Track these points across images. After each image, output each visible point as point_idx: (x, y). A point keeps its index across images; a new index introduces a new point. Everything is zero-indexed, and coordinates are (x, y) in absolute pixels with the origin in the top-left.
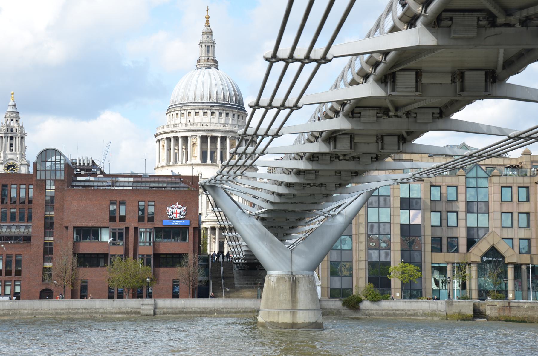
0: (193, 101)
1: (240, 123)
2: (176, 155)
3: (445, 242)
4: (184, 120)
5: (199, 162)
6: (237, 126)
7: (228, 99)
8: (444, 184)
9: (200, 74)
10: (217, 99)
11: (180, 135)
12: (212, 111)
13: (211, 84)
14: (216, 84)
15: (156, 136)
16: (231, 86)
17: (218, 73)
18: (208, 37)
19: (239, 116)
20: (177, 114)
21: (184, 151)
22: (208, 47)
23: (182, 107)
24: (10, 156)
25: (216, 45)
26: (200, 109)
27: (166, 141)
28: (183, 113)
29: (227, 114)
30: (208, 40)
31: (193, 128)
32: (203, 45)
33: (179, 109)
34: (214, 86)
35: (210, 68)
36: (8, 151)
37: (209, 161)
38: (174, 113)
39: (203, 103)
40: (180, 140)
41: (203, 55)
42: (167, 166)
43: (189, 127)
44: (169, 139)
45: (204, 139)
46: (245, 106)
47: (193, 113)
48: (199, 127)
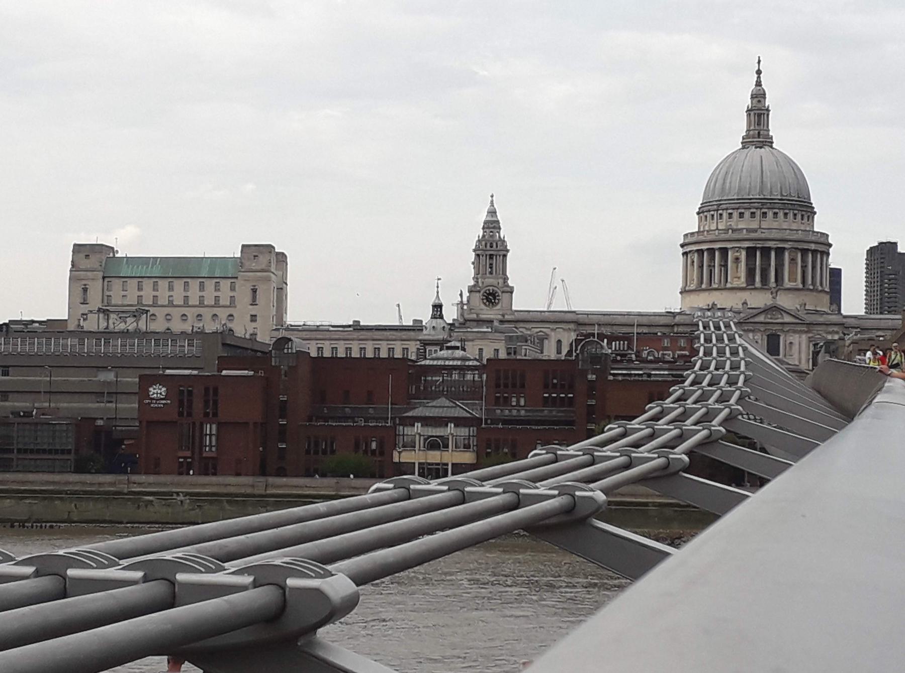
0: (735, 197)
18: (759, 101)
19: (802, 216)
20: (713, 216)
22: (759, 115)
24: (490, 281)
27: (696, 255)
29: (786, 214)
30: (759, 105)
31: (736, 236)
32: (752, 113)
34: (767, 173)
35: (761, 148)
36: (488, 275)
37: (758, 284)
38: (708, 215)
40: (717, 253)
44: (700, 252)
45: (751, 252)
46: (812, 201)
47: (736, 214)
48: (744, 235)
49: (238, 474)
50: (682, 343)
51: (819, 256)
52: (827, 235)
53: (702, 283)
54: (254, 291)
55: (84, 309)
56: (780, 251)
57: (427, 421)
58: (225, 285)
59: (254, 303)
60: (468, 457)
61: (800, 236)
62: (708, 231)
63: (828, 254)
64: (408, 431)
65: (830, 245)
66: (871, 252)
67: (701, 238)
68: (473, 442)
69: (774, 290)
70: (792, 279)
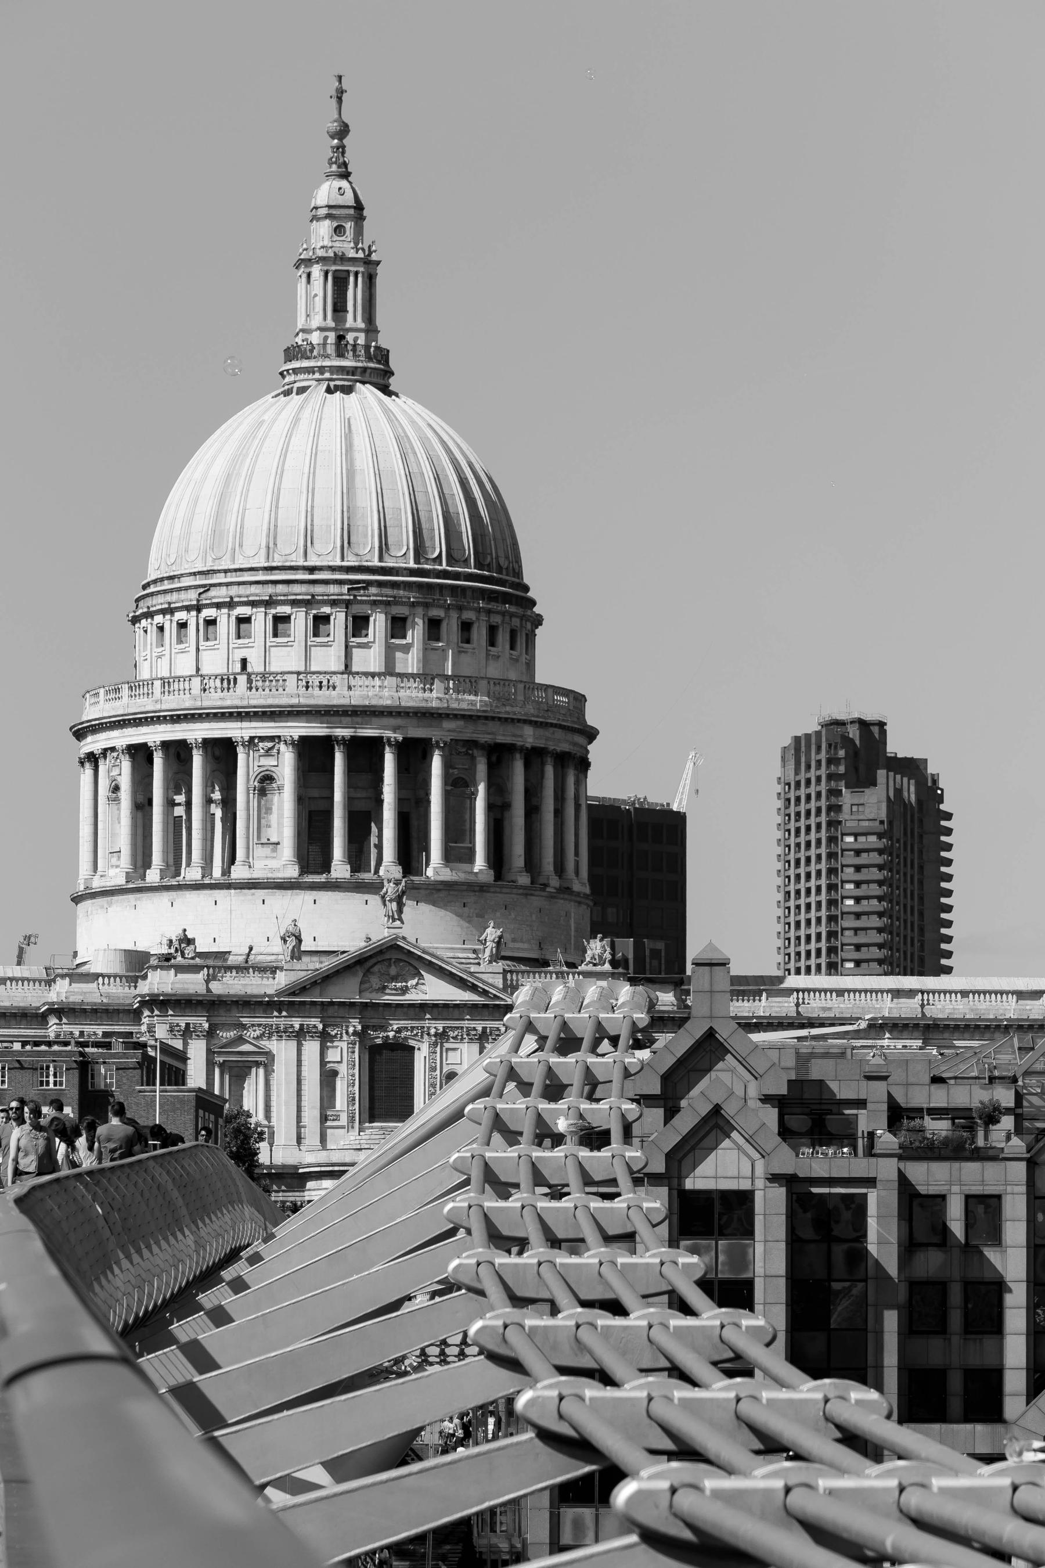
1: (494, 671)
2: (176, 828)
3: (955, 1383)
5: (292, 872)
6: (483, 684)
7: (438, 546)
8: (955, 1189)
9: (296, 420)
10: (384, 548)
11: (195, 733)
12: (356, 609)
13: (350, 474)
14: (378, 475)
15: (80, 734)
16: (453, 478)
17: (387, 411)
18: (339, 230)
19: (492, 630)
20: (183, 626)
21: (218, 813)
22: (340, 283)
23: (208, 588)
25: (380, 269)
26: (294, 603)
27: (126, 765)
28: (211, 623)
31: (259, 699)
32: (316, 271)
33: (191, 597)
34: (366, 484)
35: (348, 390)
37: (340, 869)
38: (169, 624)
39: (312, 570)
40: (197, 760)
41: (317, 321)
42: (135, 886)
44: (141, 754)
45: (313, 755)
46: (527, 580)
48: (291, 695)
51: (549, 771)
52: (579, 700)
53: (147, 864)
62: (165, 682)
63: (583, 765)
65: (591, 734)
66: (800, 749)
67: (144, 705)
69: (390, 889)
70: (457, 849)
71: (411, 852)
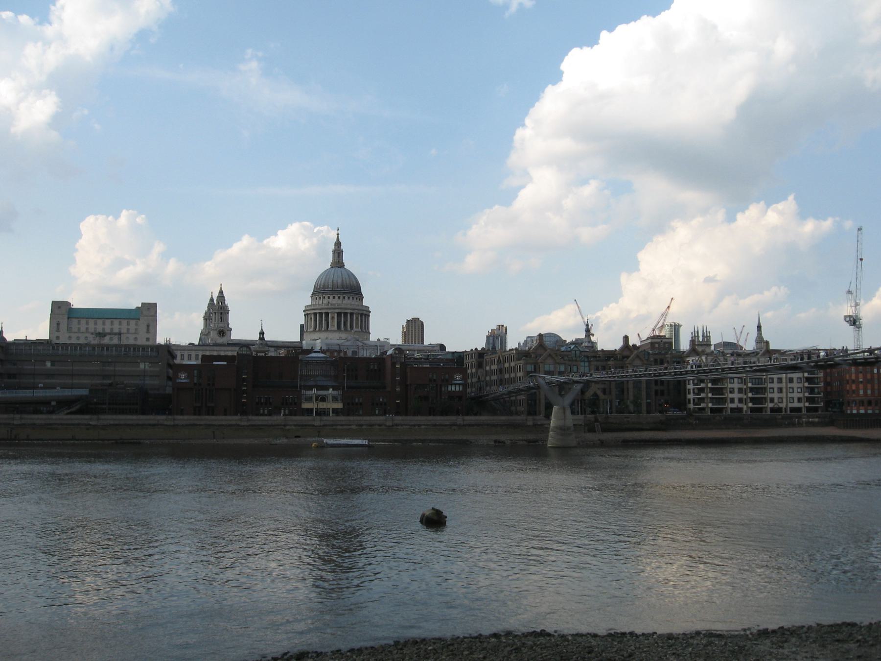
4: (325, 301)
11: (323, 311)
22: (339, 254)
24: (221, 325)
43: (330, 306)
44: (315, 314)
45: (339, 314)
49: (225, 415)
50: (336, 354)
54: (148, 326)
55: (57, 334)
56: (352, 314)
57: (320, 388)
58: (133, 322)
59: (148, 331)
60: (339, 405)
61: (360, 308)
64: (309, 393)
67: (317, 307)
68: (339, 397)
70: (357, 327)
71: (351, 327)
